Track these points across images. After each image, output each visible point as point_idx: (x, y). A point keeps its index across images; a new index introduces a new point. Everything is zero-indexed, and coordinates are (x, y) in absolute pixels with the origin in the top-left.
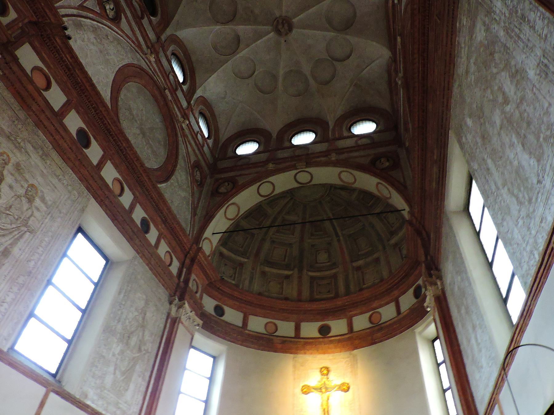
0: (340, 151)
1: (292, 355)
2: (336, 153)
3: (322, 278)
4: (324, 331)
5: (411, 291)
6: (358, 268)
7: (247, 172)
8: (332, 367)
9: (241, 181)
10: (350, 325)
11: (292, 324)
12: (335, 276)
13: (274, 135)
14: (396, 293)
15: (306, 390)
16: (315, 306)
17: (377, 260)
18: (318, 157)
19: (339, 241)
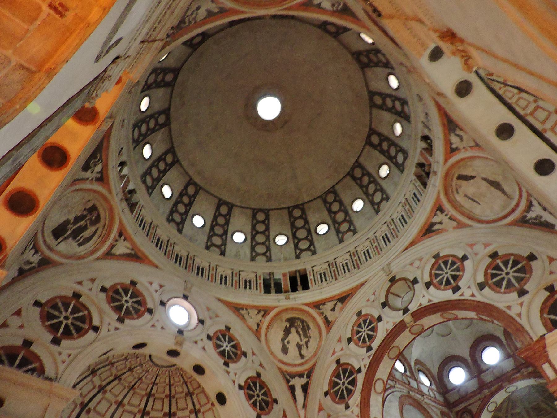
2: (524, 368)
7: (472, 401)
13: (469, 360)
18: (514, 374)
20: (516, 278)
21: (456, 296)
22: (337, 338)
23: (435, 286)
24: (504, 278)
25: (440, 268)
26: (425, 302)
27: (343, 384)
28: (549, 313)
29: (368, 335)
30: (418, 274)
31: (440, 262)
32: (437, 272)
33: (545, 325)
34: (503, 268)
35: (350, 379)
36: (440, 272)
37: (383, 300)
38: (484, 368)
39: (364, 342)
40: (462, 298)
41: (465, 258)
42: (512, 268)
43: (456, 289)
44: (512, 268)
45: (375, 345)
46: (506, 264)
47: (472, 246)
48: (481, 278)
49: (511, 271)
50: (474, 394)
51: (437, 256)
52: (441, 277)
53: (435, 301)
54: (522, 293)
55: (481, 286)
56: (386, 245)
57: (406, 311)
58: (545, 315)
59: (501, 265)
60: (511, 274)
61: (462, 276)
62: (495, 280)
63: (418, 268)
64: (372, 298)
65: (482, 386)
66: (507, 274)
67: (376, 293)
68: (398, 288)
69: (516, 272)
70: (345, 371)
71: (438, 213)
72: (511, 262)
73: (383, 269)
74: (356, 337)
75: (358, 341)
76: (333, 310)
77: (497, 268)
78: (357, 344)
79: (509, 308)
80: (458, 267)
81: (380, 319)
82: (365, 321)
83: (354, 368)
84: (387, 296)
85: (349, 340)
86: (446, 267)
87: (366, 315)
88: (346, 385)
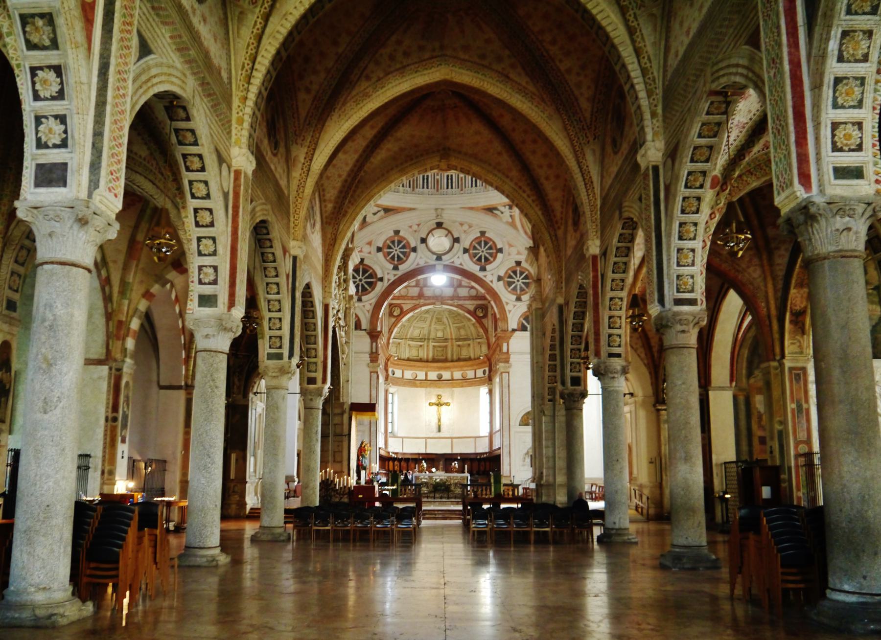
0: (460, 298)
1: (424, 389)
3: (439, 347)
4: (440, 378)
5: (483, 370)
6: (459, 346)
8: (443, 395)
9: (405, 308)
10: (452, 375)
11: (424, 373)
12: (446, 347)
14: (475, 367)
15: (431, 404)
16: (435, 365)
17: (469, 345)
19: (450, 328)
20: (521, 287)
21: (481, 274)
22: (367, 240)
23: (470, 255)
24: (514, 282)
25: (479, 244)
26: (457, 264)
27: (361, 280)
28: (524, 319)
29: (398, 256)
30: (463, 237)
31: (483, 239)
32: (476, 245)
33: (518, 325)
34: (518, 275)
35: (369, 280)
36: (478, 247)
37: (424, 237)
38: (429, 284)
39: (393, 258)
40: (484, 279)
41: (500, 250)
42: (523, 279)
43: (483, 269)
44: (523, 279)
45: (404, 268)
46: (521, 273)
47: (510, 246)
48: (502, 274)
49: (521, 281)
50: (412, 298)
51: (483, 233)
52: (477, 251)
53: (465, 267)
54: (519, 299)
55: (500, 279)
56: (447, 188)
57: (439, 258)
58: (521, 319)
59: (518, 272)
60: (520, 283)
61: (491, 263)
62: (509, 280)
63: (465, 231)
64: (415, 227)
65: (421, 296)
66: (518, 281)
67: (420, 226)
68: (439, 232)
69: (523, 283)
70: (365, 272)
71: (507, 207)
72: (524, 275)
73: (436, 209)
74: (386, 250)
75: (386, 254)
76: (375, 214)
77: (515, 272)
78: (385, 257)
79: (507, 304)
80: (492, 253)
81: (414, 250)
82: (399, 242)
83: (376, 275)
84: (428, 234)
85: (379, 249)
86: (485, 247)
87: (402, 237)
88: (363, 282)
